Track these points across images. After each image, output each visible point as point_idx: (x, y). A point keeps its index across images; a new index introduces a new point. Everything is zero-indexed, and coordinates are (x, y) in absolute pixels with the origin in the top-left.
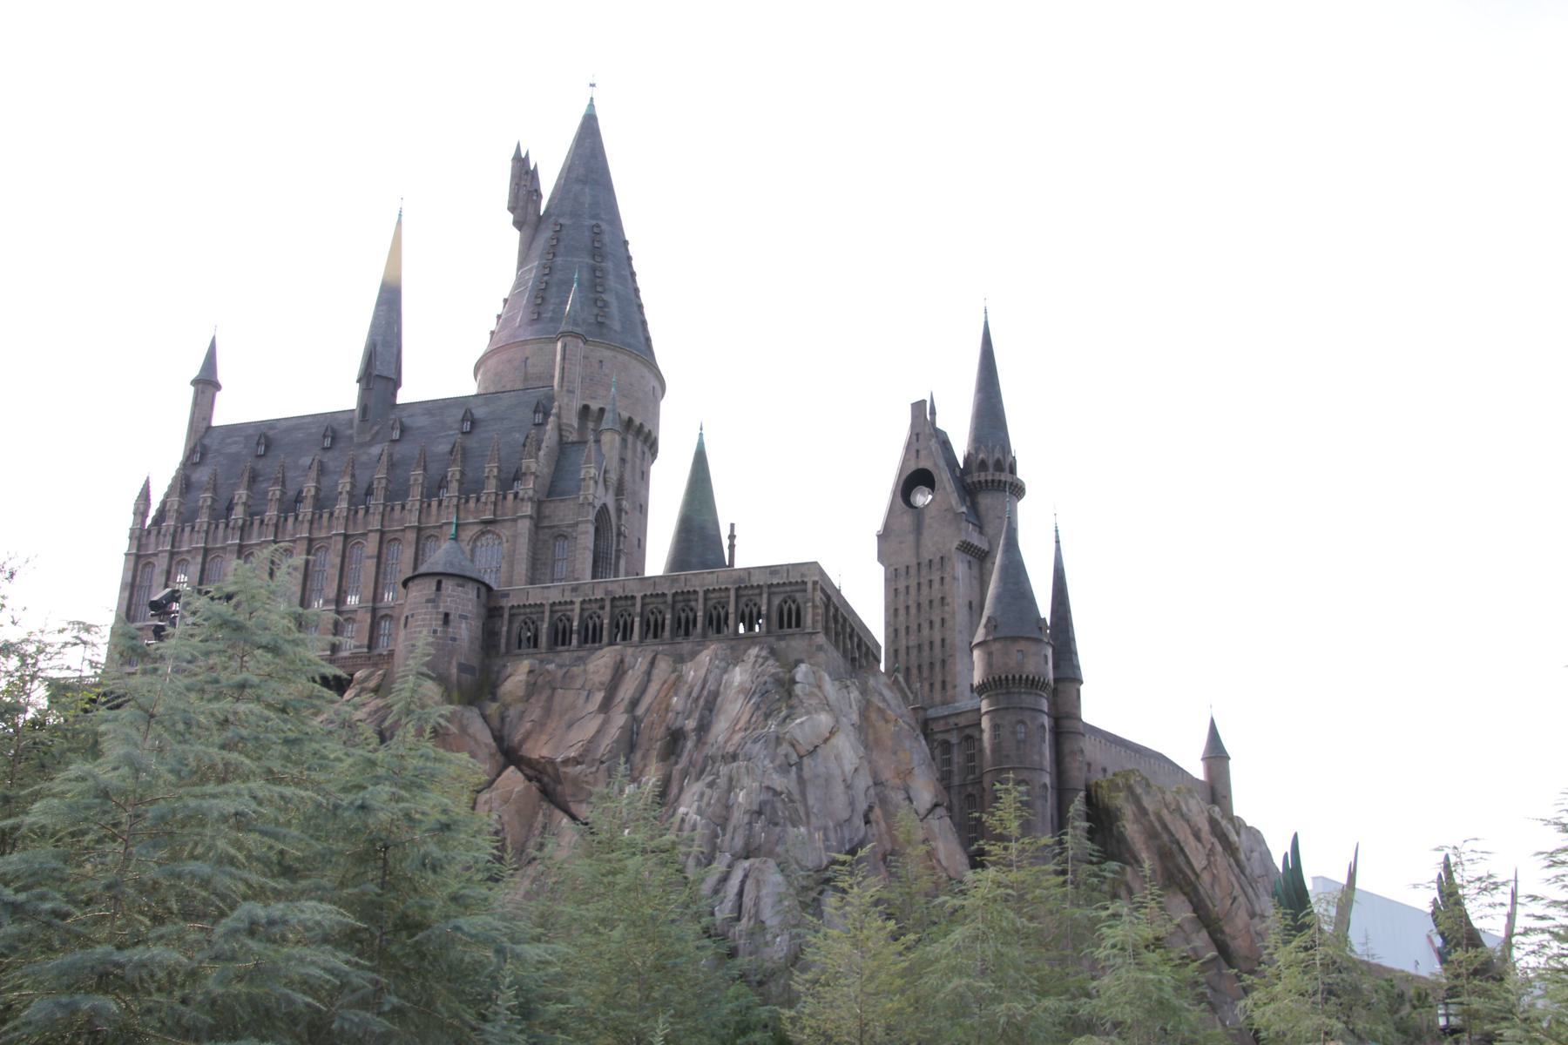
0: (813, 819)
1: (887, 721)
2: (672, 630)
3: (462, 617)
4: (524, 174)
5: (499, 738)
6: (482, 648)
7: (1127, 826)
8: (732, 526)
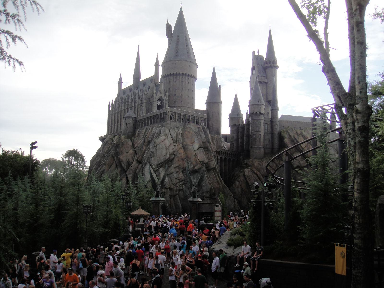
0: (157, 156)
1: (190, 133)
2: (153, 122)
3: (129, 124)
4: (168, 27)
5: (133, 143)
6: (133, 128)
7: (285, 139)
8: (220, 85)
